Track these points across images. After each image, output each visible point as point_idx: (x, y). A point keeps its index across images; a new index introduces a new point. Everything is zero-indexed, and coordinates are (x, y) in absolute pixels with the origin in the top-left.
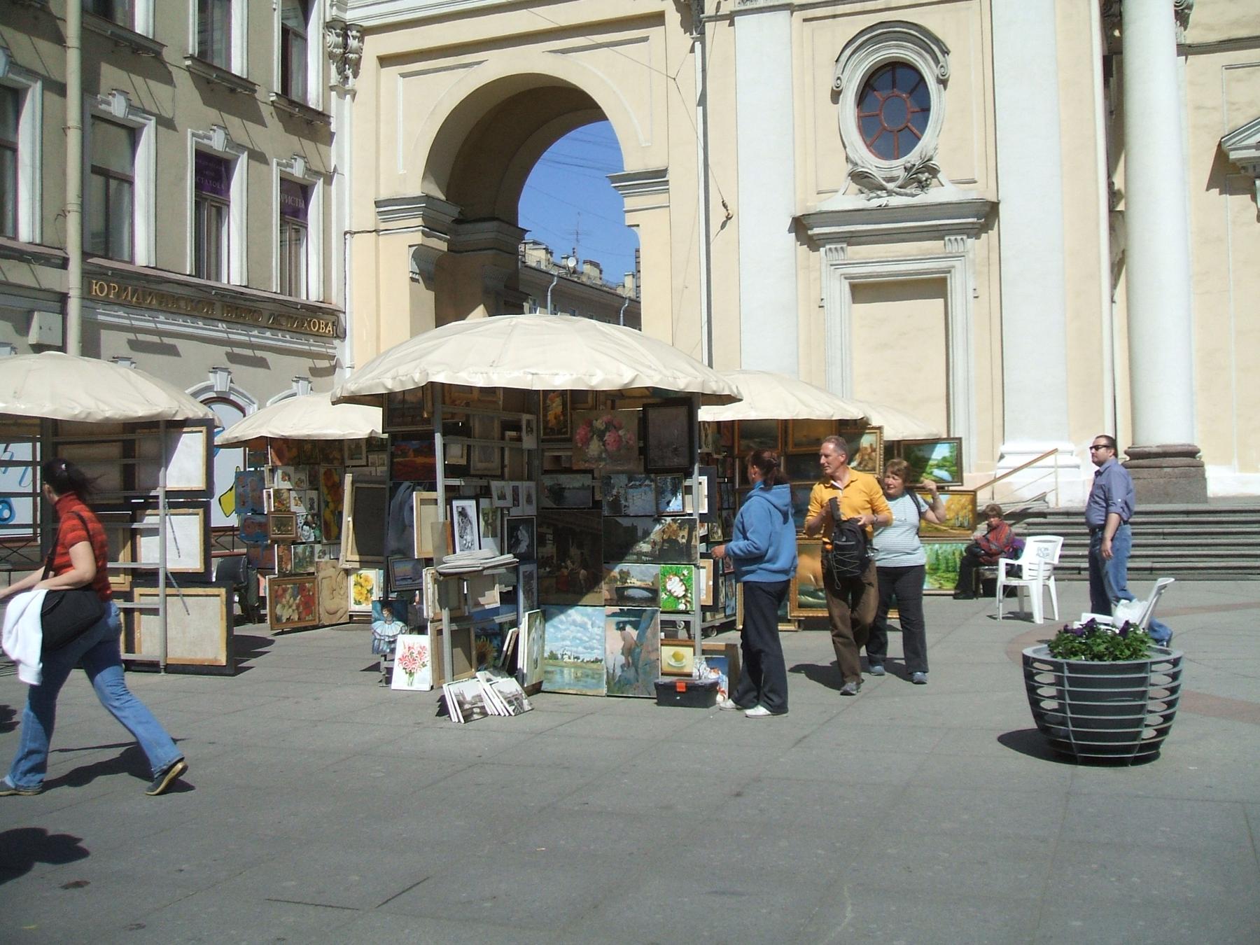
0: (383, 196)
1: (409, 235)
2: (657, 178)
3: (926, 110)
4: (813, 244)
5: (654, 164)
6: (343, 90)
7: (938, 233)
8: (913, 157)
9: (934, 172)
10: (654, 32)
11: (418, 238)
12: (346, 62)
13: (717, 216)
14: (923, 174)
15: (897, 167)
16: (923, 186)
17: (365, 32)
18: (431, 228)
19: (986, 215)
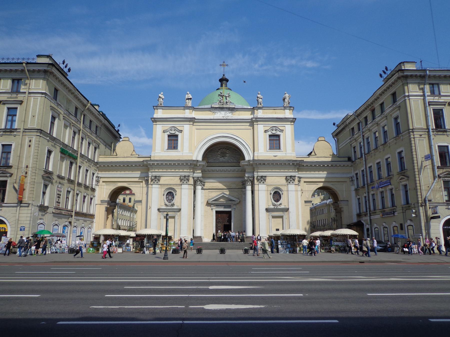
0: (102, 199)
1: (106, 205)
2: (140, 201)
3: (174, 198)
4: (160, 212)
5: (140, 199)
6: (97, 185)
7: (174, 212)
8: (172, 203)
10: (141, 184)
11: (106, 206)
12: (98, 181)
13: (148, 208)
14: (173, 205)
15: (170, 204)
17: (101, 178)
18: (108, 204)
19: (180, 210)
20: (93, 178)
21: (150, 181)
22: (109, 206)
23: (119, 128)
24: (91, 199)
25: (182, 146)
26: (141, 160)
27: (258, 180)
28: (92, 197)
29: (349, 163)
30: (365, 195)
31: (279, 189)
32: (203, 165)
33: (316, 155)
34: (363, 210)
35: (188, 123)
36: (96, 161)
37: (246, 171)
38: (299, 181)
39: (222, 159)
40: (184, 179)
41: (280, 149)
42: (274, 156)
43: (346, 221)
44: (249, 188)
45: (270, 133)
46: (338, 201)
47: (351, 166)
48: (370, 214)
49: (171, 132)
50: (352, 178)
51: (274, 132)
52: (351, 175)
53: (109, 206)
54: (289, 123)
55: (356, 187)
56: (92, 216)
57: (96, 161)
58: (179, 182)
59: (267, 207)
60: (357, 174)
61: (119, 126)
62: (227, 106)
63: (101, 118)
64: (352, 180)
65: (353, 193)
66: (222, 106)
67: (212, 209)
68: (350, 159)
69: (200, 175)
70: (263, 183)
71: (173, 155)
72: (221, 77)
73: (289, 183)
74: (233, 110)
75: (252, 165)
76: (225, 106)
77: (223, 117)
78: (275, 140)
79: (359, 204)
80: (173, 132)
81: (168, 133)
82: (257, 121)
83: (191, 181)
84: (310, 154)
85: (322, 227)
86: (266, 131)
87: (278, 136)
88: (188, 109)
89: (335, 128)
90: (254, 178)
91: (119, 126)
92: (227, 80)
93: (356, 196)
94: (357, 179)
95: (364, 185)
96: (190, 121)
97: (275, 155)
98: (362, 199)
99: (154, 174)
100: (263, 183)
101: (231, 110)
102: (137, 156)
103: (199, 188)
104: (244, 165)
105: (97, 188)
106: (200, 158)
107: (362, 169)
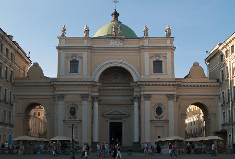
9: (77, 117)
14: (75, 118)
16: (75, 119)
20: (10, 96)
21: (56, 98)
22: (24, 118)
23: (30, 55)
24: (10, 112)
25: (82, 70)
26: (49, 81)
27: (144, 97)
28: (11, 111)
29: (218, 84)
30: (229, 109)
31: (161, 104)
32: (100, 85)
33: (191, 77)
34: (227, 122)
35: (87, 50)
36: (12, 82)
37: (135, 90)
38: (177, 98)
39: (114, 81)
40: (84, 97)
41: (162, 72)
42: (157, 78)
43: (213, 129)
44: (136, 104)
45: (154, 59)
46: (208, 114)
47: (220, 86)
48: (232, 124)
49: (72, 58)
50: (219, 96)
51: (158, 58)
52: (220, 94)
53: (24, 118)
54: (170, 51)
55: (222, 103)
56: (12, 126)
57: (12, 82)
58: (80, 99)
59: (151, 119)
60: (223, 93)
61: (30, 53)
62: (119, 37)
63: (15, 47)
64: (219, 98)
65: (220, 108)
66: (114, 37)
67: (107, 121)
68: (218, 81)
69: (97, 94)
70: (148, 99)
71: (74, 76)
72: (113, 11)
73: (170, 100)
74: (124, 40)
75: (139, 85)
76: (117, 37)
77: (116, 46)
78: (158, 66)
79: (224, 116)
80: (74, 58)
81: (71, 60)
82: (144, 49)
83: (90, 99)
84: (187, 76)
85: (194, 135)
86: (151, 57)
87: (161, 62)
88: (86, 39)
89: (207, 55)
90: (140, 96)
91: (30, 53)
92: (118, 15)
93: (222, 110)
94: (223, 96)
95: (229, 101)
96: (88, 49)
97: (159, 77)
98: (227, 112)
99: (60, 93)
100: (148, 99)
101: (123, 40)
102: (46, 78)
103: (96, 104)
104: (132, 85)
105: (14, 104)
106: (97, 79)
107: (228, 89)
